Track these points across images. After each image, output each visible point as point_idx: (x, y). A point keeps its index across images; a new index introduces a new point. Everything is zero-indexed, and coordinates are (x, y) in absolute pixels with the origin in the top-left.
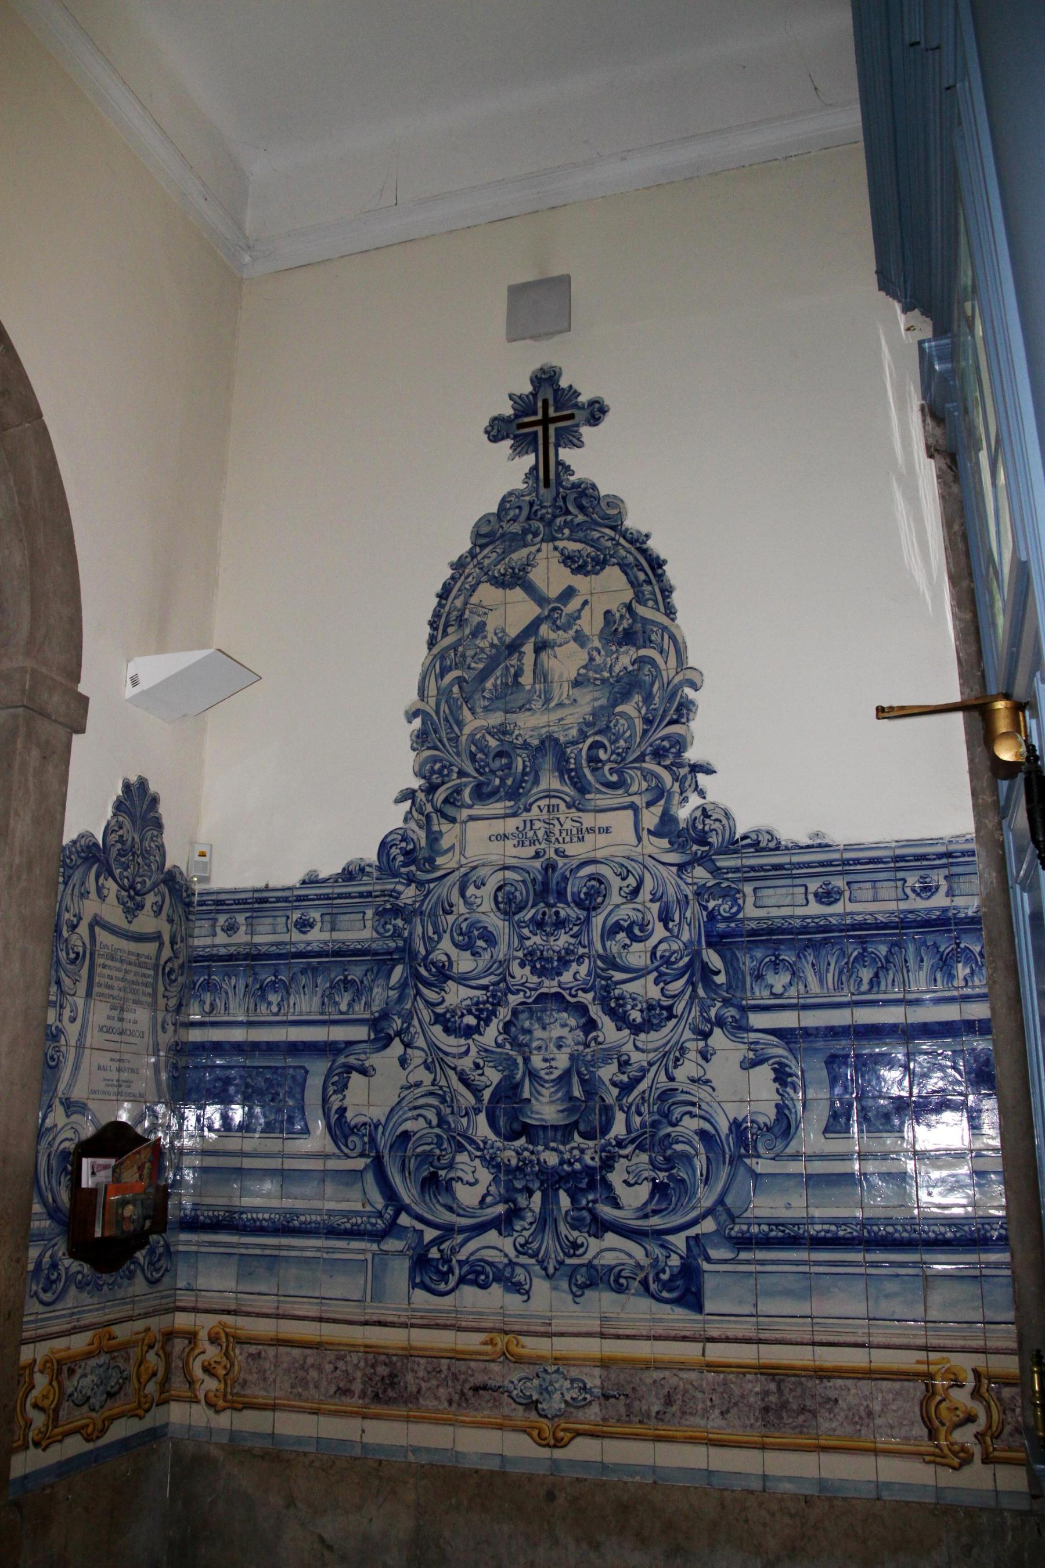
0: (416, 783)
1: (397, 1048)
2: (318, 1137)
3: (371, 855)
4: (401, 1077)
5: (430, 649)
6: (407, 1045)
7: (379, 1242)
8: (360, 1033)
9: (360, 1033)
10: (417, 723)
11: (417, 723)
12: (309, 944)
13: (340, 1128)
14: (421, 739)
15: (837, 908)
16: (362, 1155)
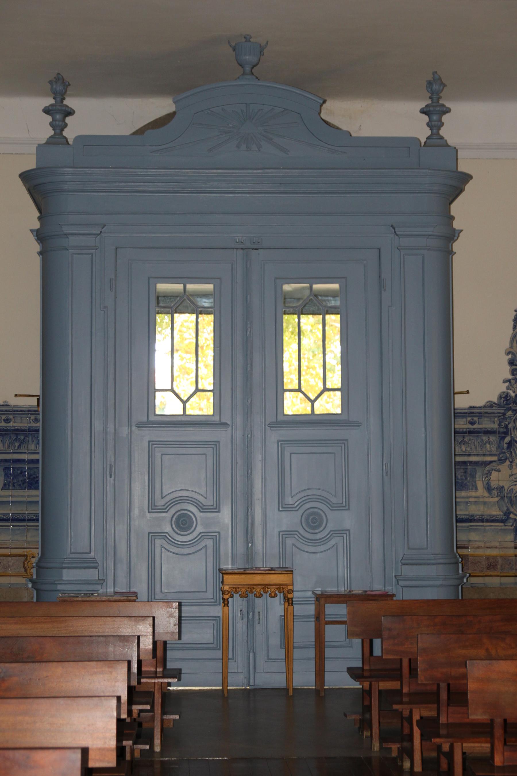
0: (510, 377)
1: (508, 463)
2: (481, 491)
3: (495, 400)
4: (509, 472)
5: (514, 331)
6: (511, 462)
7: (504, 523)
8: (495, 458)
9: (495, 458)
10: (510, 356)
11: (510, 356)
12: (474, 429)
13: (489, 489)
14: (511, 363)
15: (475, 426)
16: (497, 497)
